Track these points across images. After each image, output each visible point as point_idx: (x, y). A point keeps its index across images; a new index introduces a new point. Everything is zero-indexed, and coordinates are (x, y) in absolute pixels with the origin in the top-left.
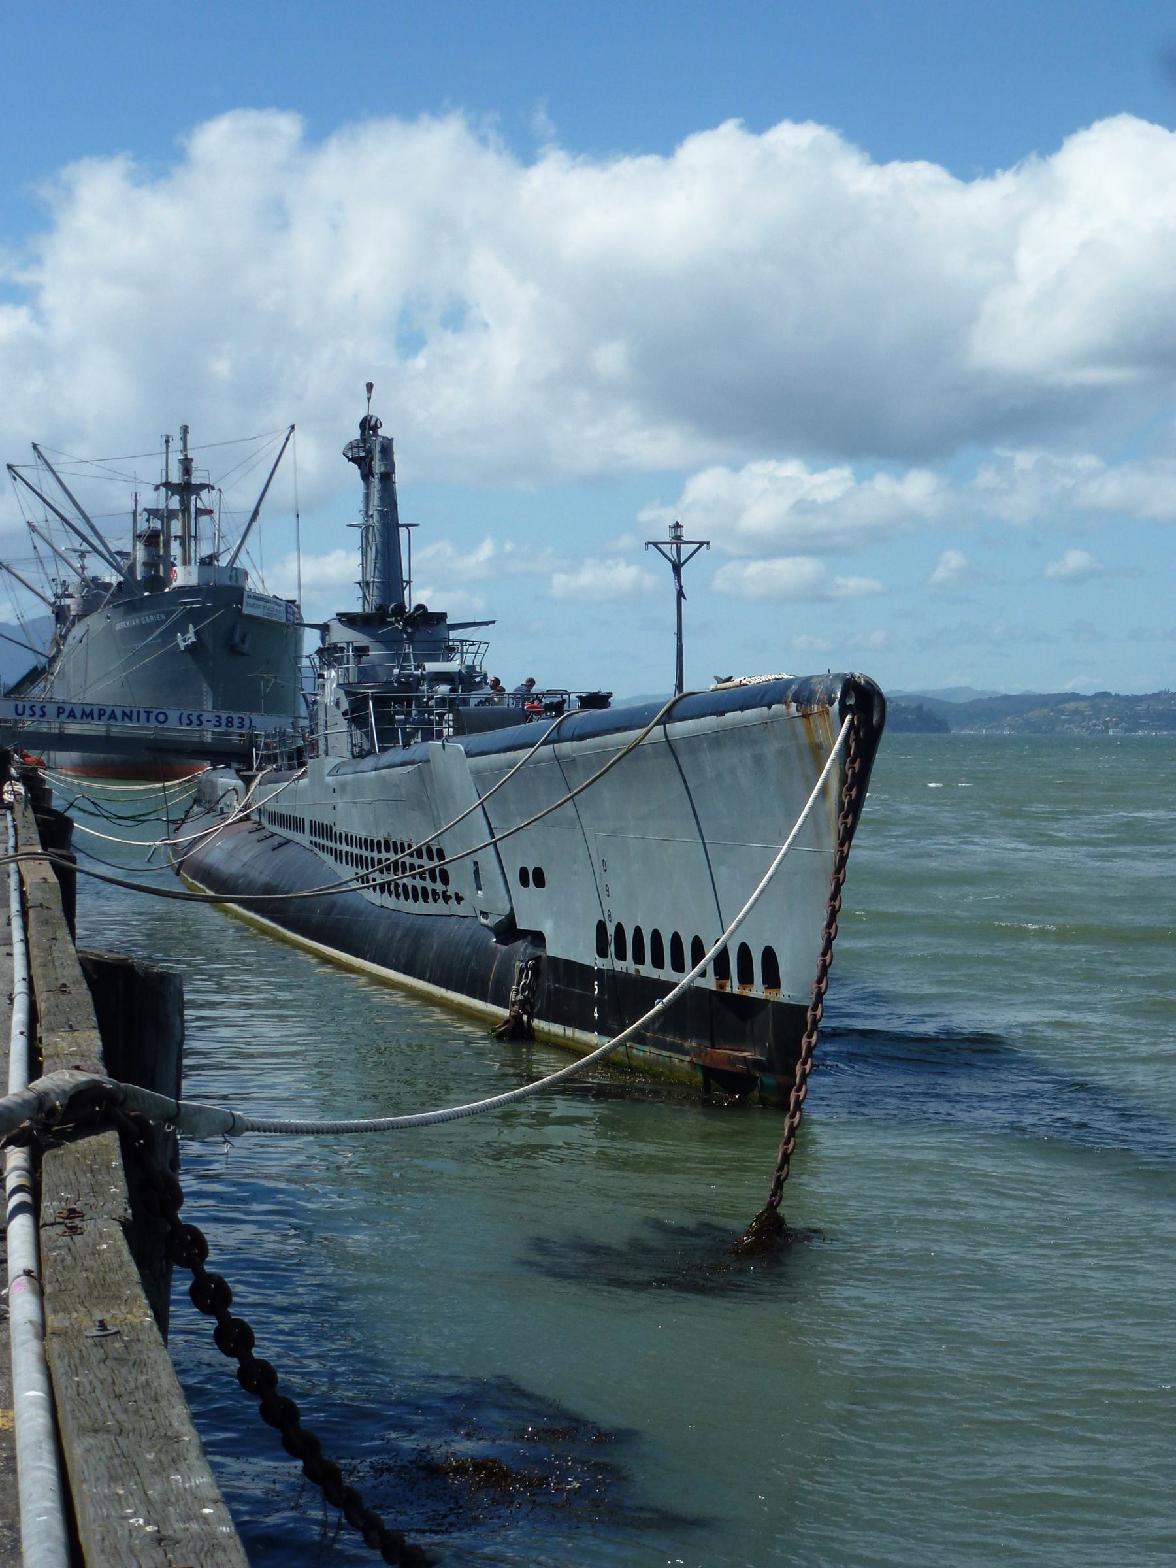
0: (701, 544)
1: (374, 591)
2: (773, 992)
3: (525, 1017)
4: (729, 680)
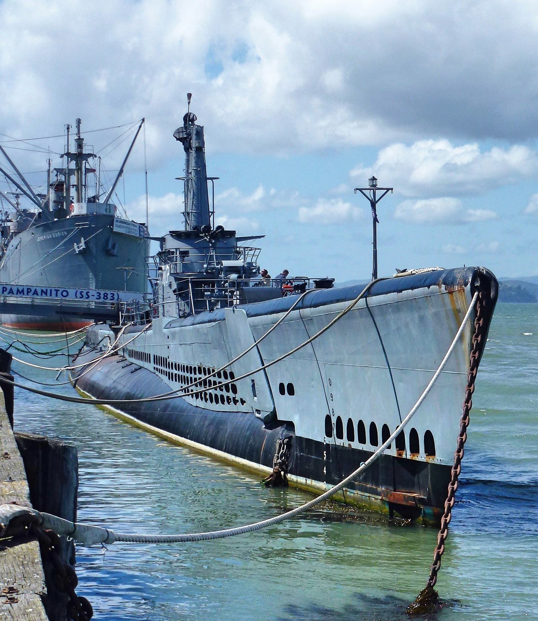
0: (388, 190)
2: (431, 458)
3: (282, 473)
4: (404, 271)
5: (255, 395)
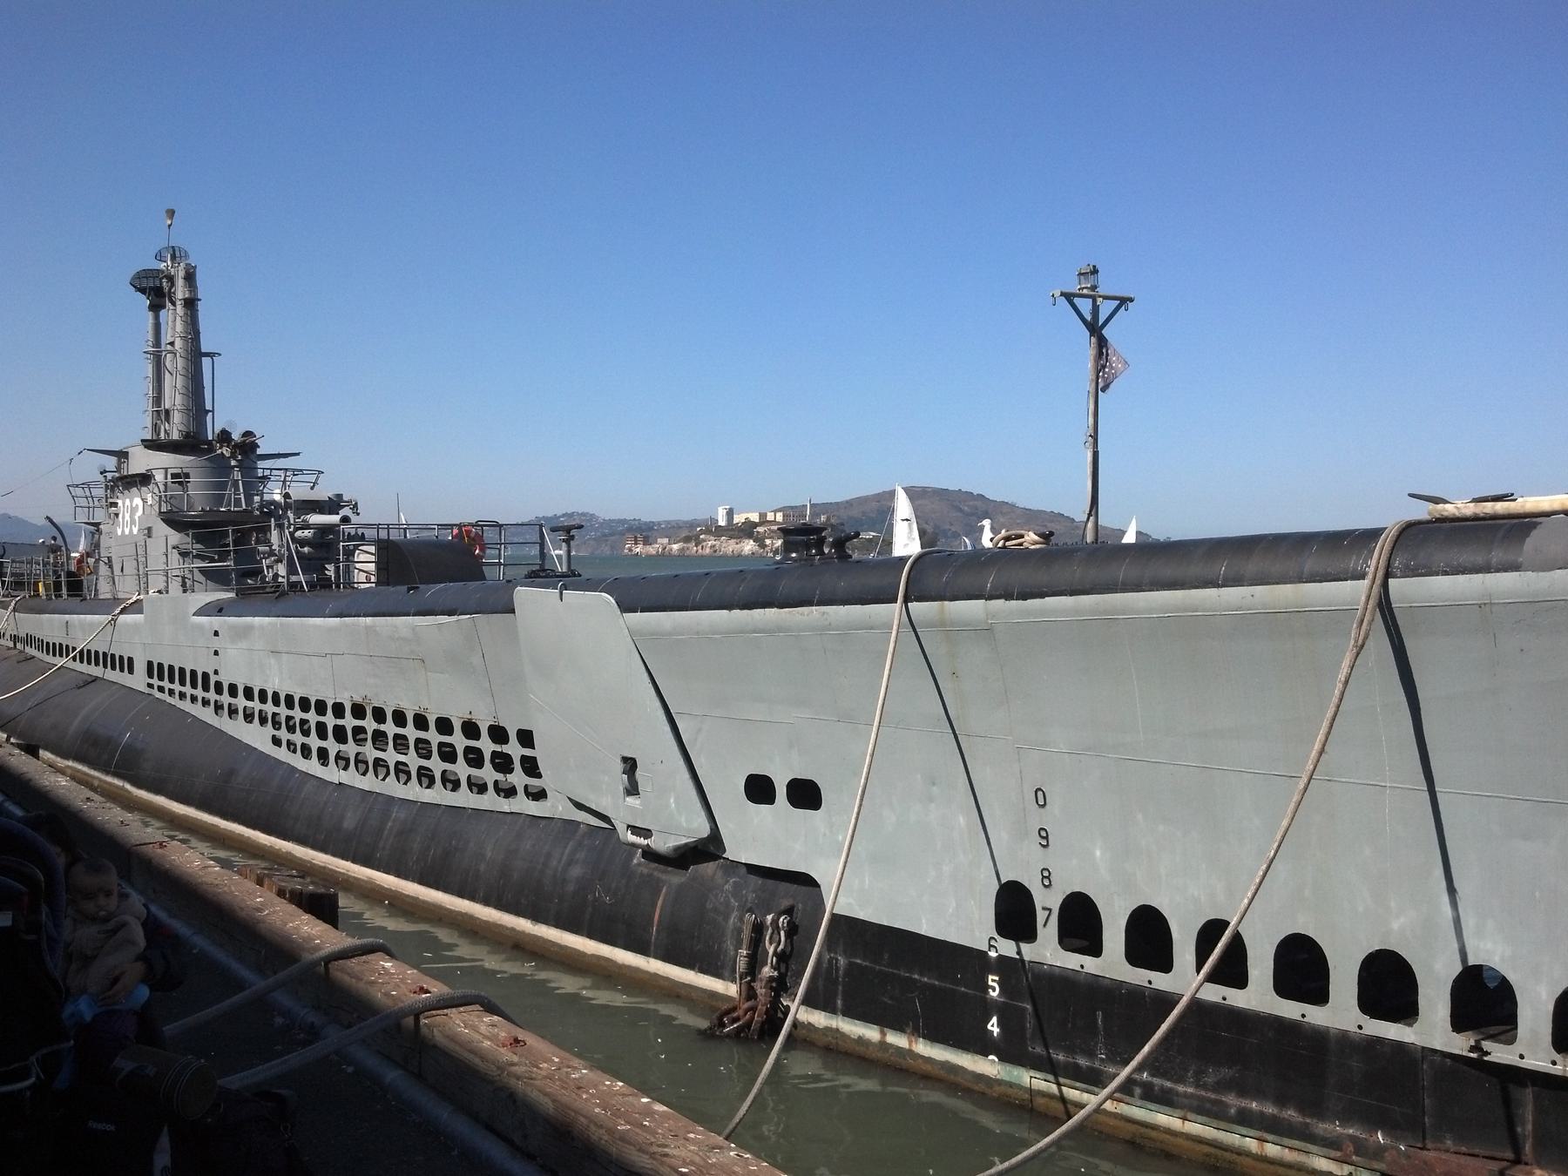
1: (177, 417)
5: (632, 790)
